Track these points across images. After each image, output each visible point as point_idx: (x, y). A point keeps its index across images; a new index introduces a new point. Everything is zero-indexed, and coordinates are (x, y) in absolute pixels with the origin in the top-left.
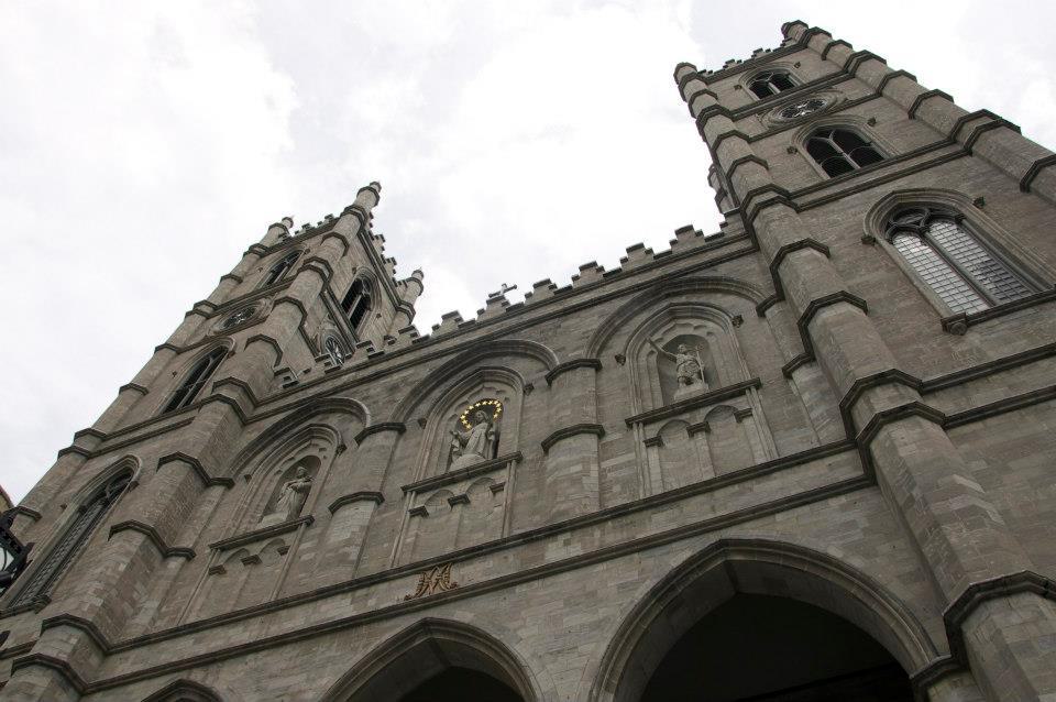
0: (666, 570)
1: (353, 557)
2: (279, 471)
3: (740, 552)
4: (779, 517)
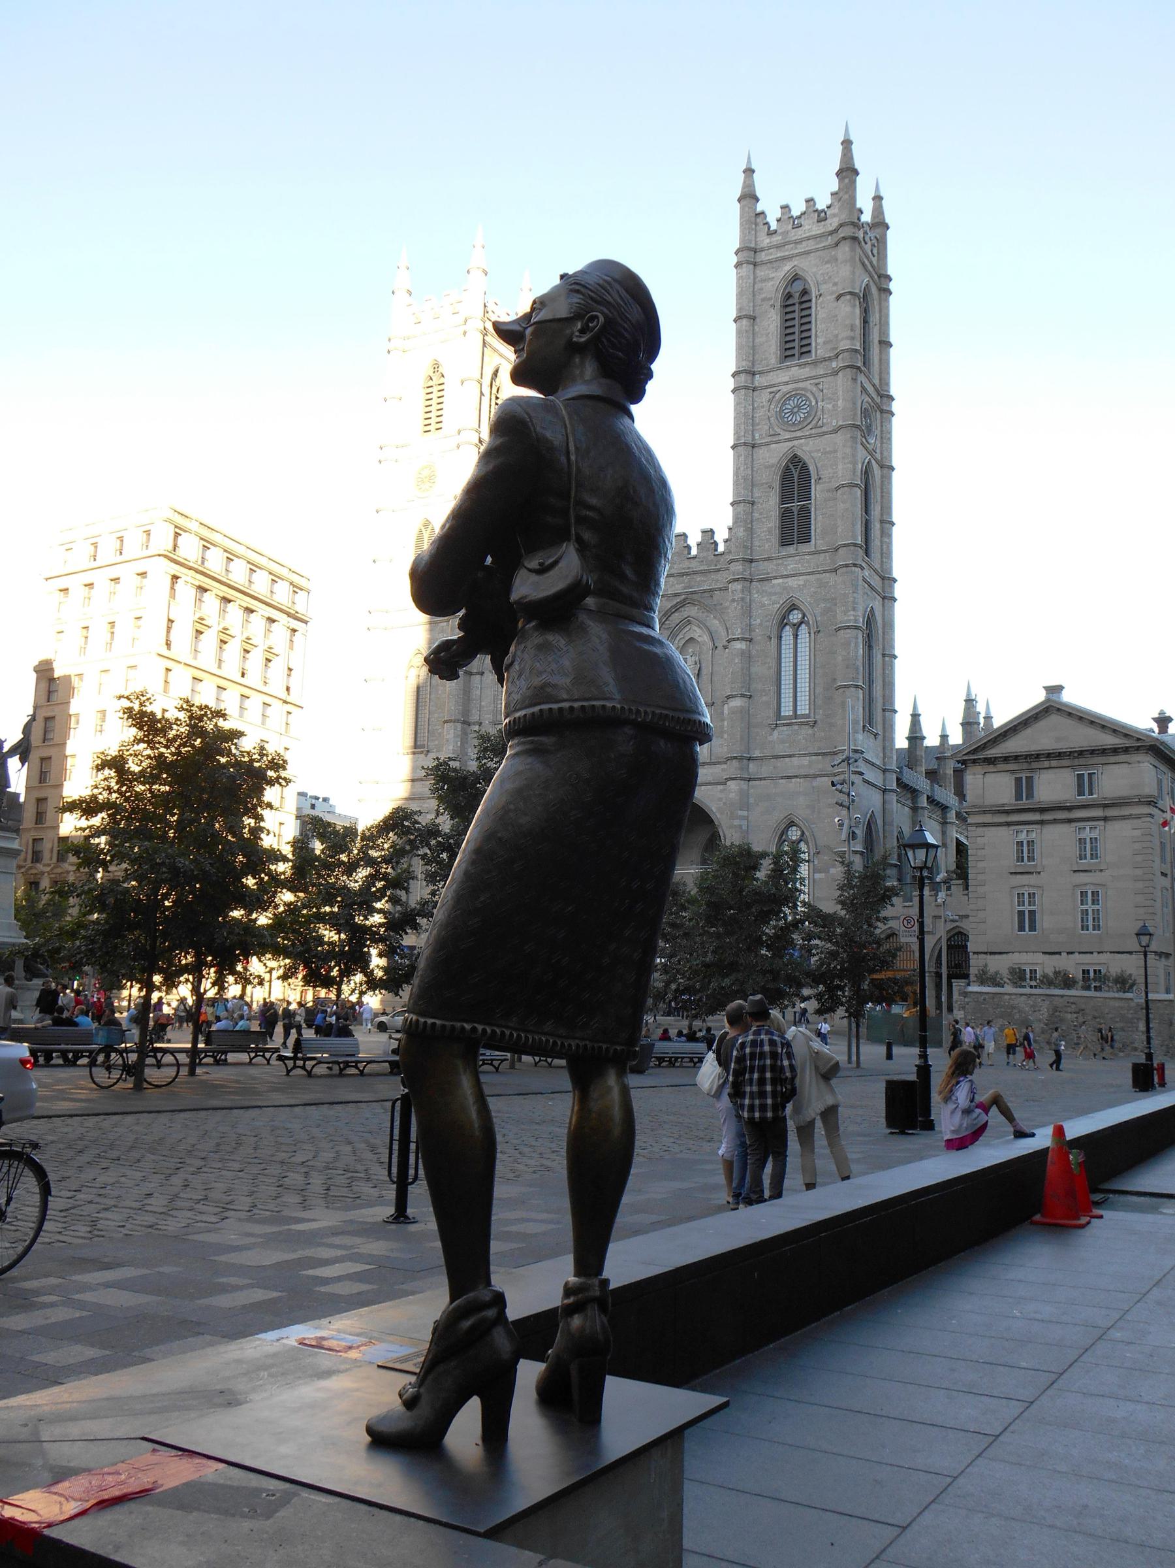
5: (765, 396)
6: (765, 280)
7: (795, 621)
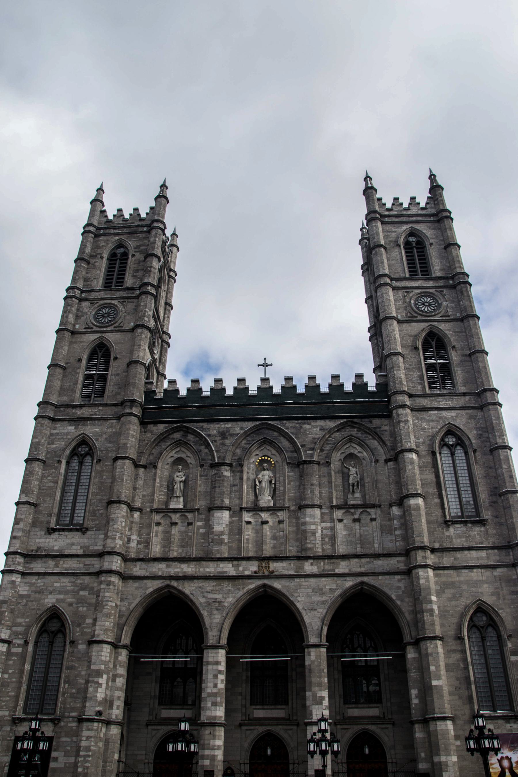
0: (345, 588)
1: (226, 541)
2: (168, 464)
3: (366, 586)
4: (380, 577)
5: (400, 293)
6: (390, 232)
7: (451, 443)
